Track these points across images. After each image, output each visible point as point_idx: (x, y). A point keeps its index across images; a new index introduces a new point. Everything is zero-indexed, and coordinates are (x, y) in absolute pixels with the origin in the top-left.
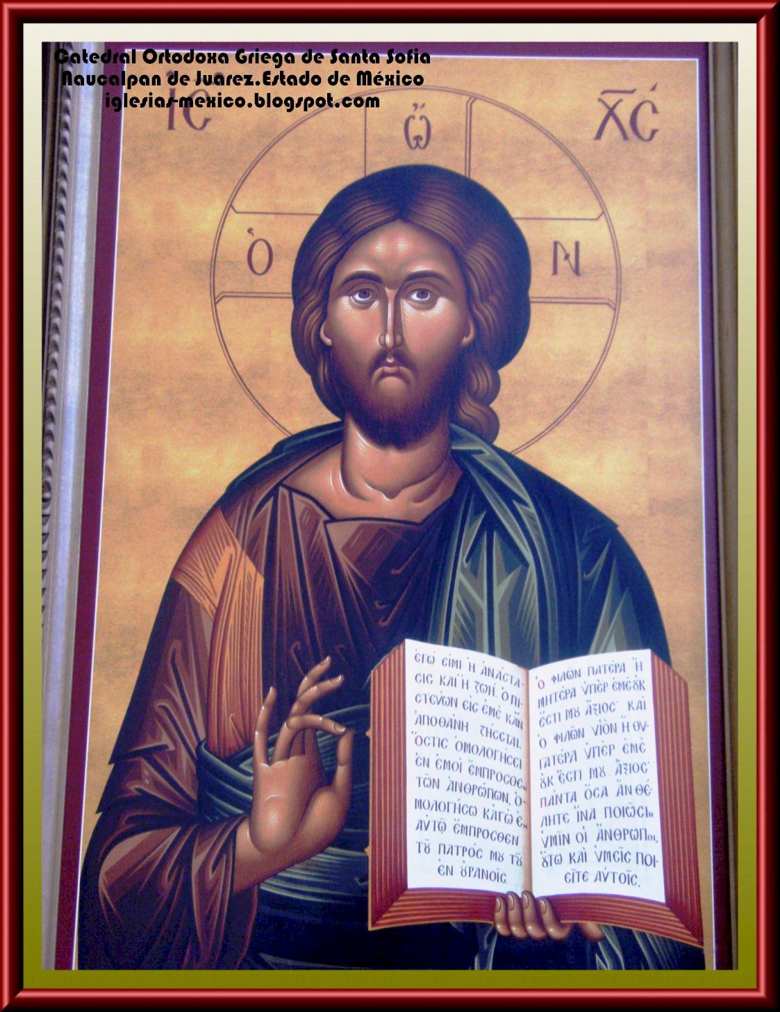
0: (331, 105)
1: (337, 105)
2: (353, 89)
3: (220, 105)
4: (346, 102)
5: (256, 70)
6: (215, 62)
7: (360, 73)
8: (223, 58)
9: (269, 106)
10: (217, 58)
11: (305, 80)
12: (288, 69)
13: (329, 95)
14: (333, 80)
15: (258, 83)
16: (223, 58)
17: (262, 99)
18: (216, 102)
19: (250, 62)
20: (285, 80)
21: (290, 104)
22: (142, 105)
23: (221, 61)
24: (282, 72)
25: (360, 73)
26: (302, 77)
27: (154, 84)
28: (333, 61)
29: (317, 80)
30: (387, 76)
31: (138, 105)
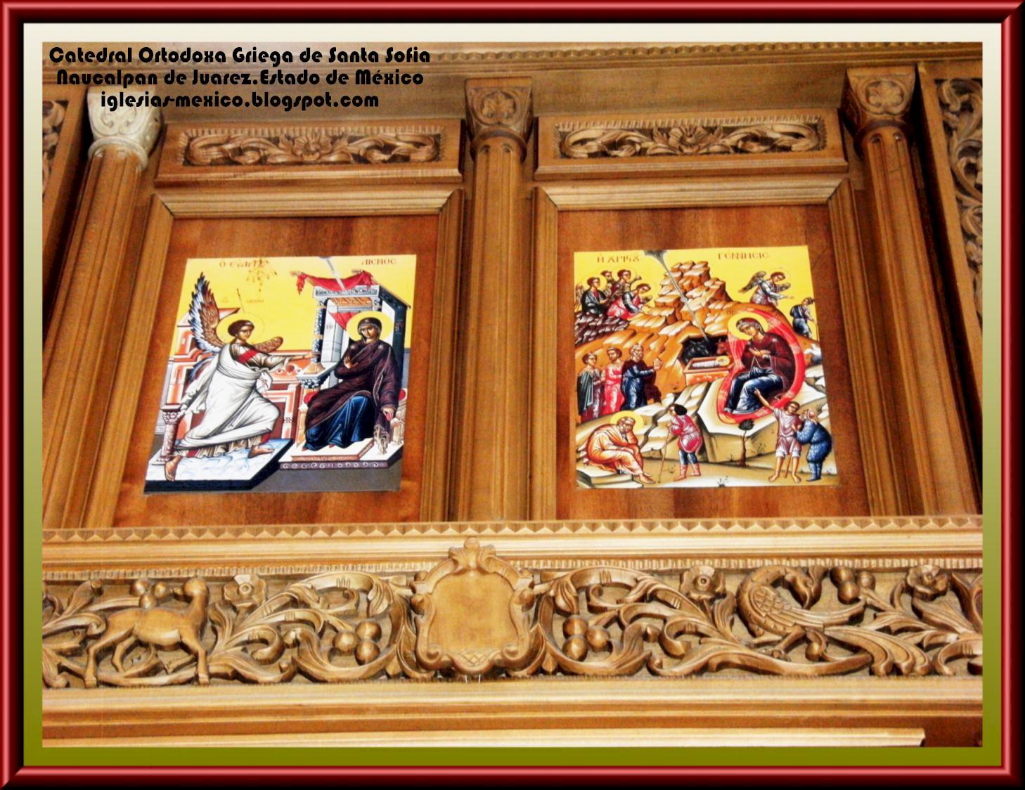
0: (329, 104)
1: (336, 104)
2: (353, 90)
3: (217, 104)
4: (345, 101)
7: (359, 72)
8: (220, 57)
9: (266, 105)
13: (327, 94)
14: (331, 79)
15: (255, 82)
16: (220, 57)
17: (259, 98)
18: (213, 101)
20: (283, 79)
21: (288, 103)
22: (139, 105)
24: (280, 71)
28: (332, 60)
29: (315, 79)
30: (386, 75)
31: (134, 104)
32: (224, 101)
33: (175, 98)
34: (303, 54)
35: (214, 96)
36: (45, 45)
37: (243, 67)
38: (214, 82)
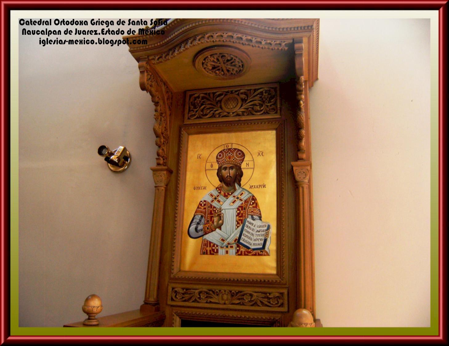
3: (84, 44)
5: (99, 28)
6: (82, 25)
7: (140, 29)
8: (86, 23)
9: (104, 44)
10: (83, 23)
11: (118, 32)
12: (111, 28)
15: (99, 34)
16: (86, 23)
17: (101, 41)
18: (83, 42)
19: (96, 25)
20: (110, 32)
21: (112, 43)
22: (54, 43)
23: (85, 24)
24: (109, 29)
25: (140, 29)
26: (117, 31)
27: (58, 34)
28: (129, 24)
31: (52, 43)
32: (87, 42)
33: (68, 40)
34: (118, 22)
35: (83, 40)
36: (19, 19)
37: (94, 28)
38: (83, 34)
